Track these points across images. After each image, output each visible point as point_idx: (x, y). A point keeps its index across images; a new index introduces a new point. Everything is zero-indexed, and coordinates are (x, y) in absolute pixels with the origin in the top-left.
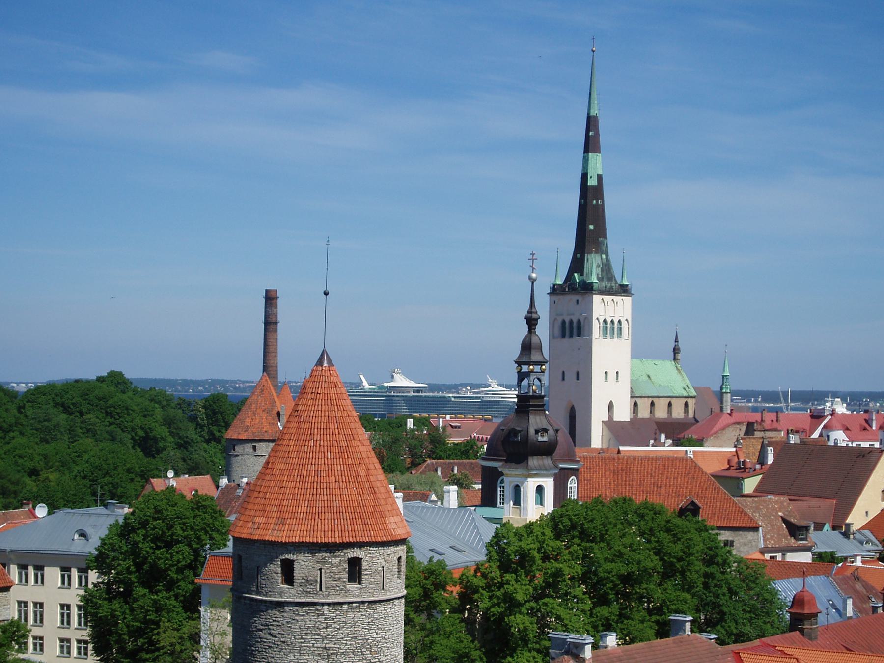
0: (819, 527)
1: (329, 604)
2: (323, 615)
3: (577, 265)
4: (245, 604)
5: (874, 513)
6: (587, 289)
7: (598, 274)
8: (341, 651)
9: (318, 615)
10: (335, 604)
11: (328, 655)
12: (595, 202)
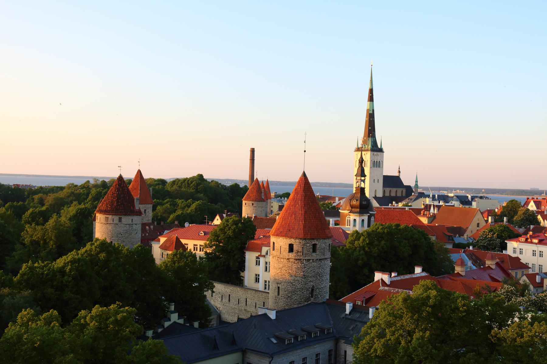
0: (455, 236)
1: (305, 260)
2: (303, 263)
3: (365, 142)
4: (276, 259)
7: (372, 145)
8: (309, 276)
9: (302, 264)
10: (308, 259)
11: (305, 278)
12: (371, 119)
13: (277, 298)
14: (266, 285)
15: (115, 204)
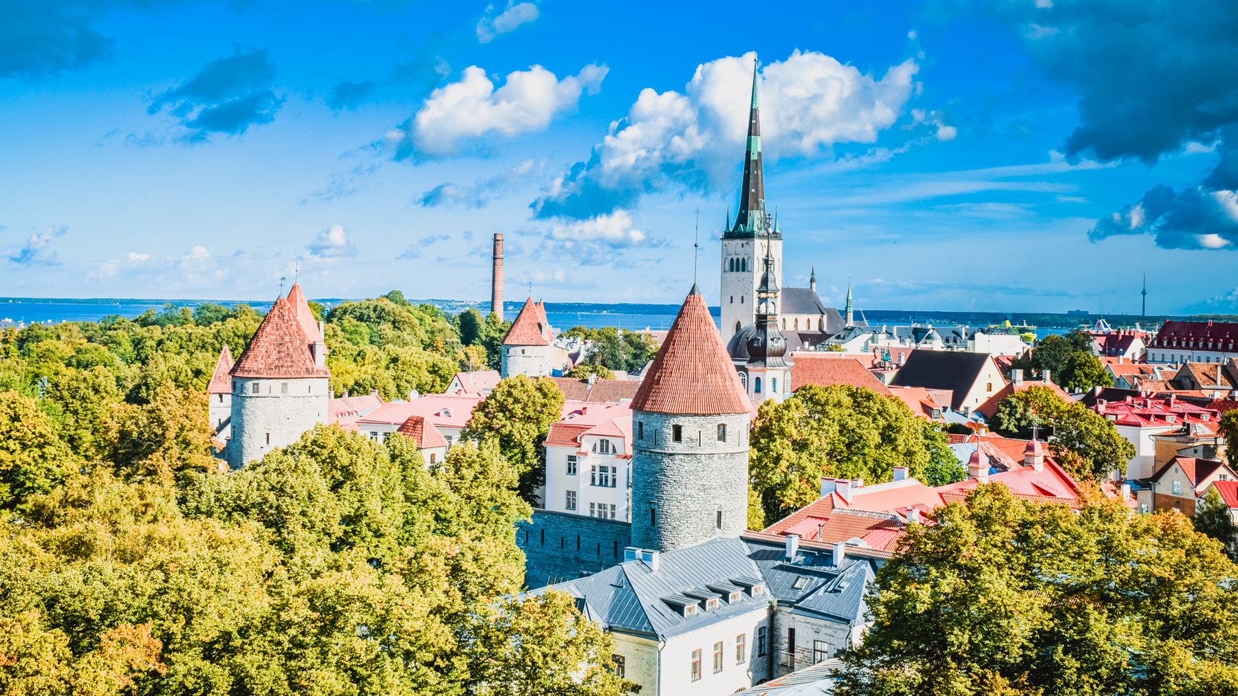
3: (743, 218)
5: (982, 401)
6: (749, 236)
13: (651, 530)
14: (592, 512)
15: (274, 355)
